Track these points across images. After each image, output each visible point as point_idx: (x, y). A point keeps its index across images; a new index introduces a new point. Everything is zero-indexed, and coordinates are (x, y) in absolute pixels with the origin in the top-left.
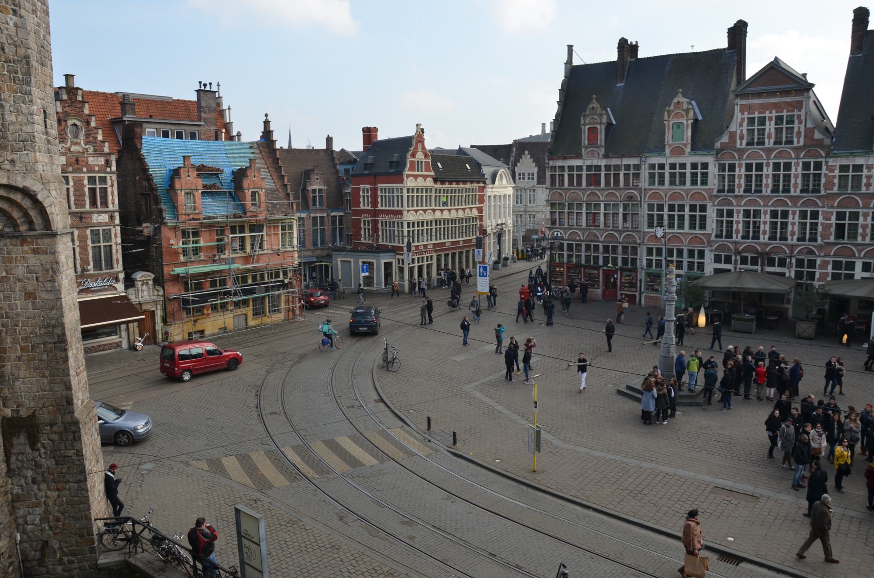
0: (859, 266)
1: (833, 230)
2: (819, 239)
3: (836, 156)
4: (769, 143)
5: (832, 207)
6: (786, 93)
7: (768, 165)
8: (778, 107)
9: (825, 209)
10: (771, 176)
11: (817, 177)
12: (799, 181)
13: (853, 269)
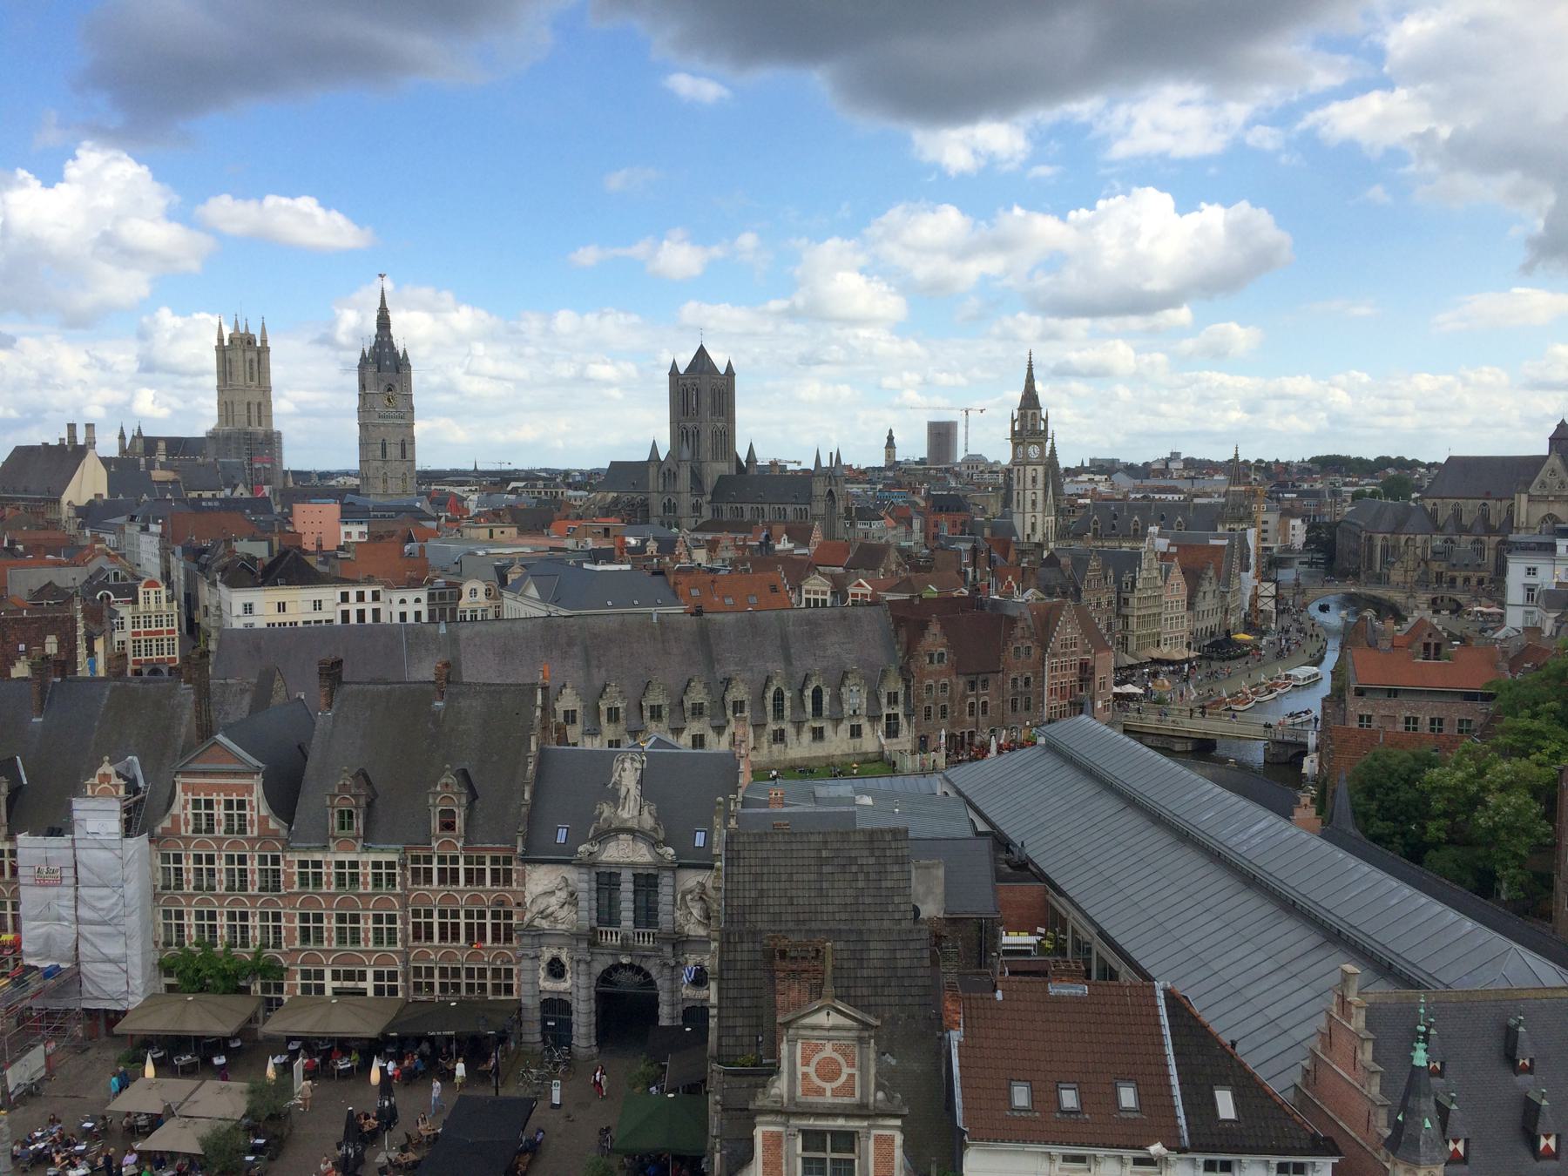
0: (328, 974)
1: (297, 934)
2: (284, 944)
3: (292, 850)
4: (220, 831)
5: (294, 908)
6: (235, 774)
7: (220, 858)
8: (226, 789)
9: (287, 911)
10: (224, 870)
11: (276, 873)
12: (256, 877)
13: (323, 979)
